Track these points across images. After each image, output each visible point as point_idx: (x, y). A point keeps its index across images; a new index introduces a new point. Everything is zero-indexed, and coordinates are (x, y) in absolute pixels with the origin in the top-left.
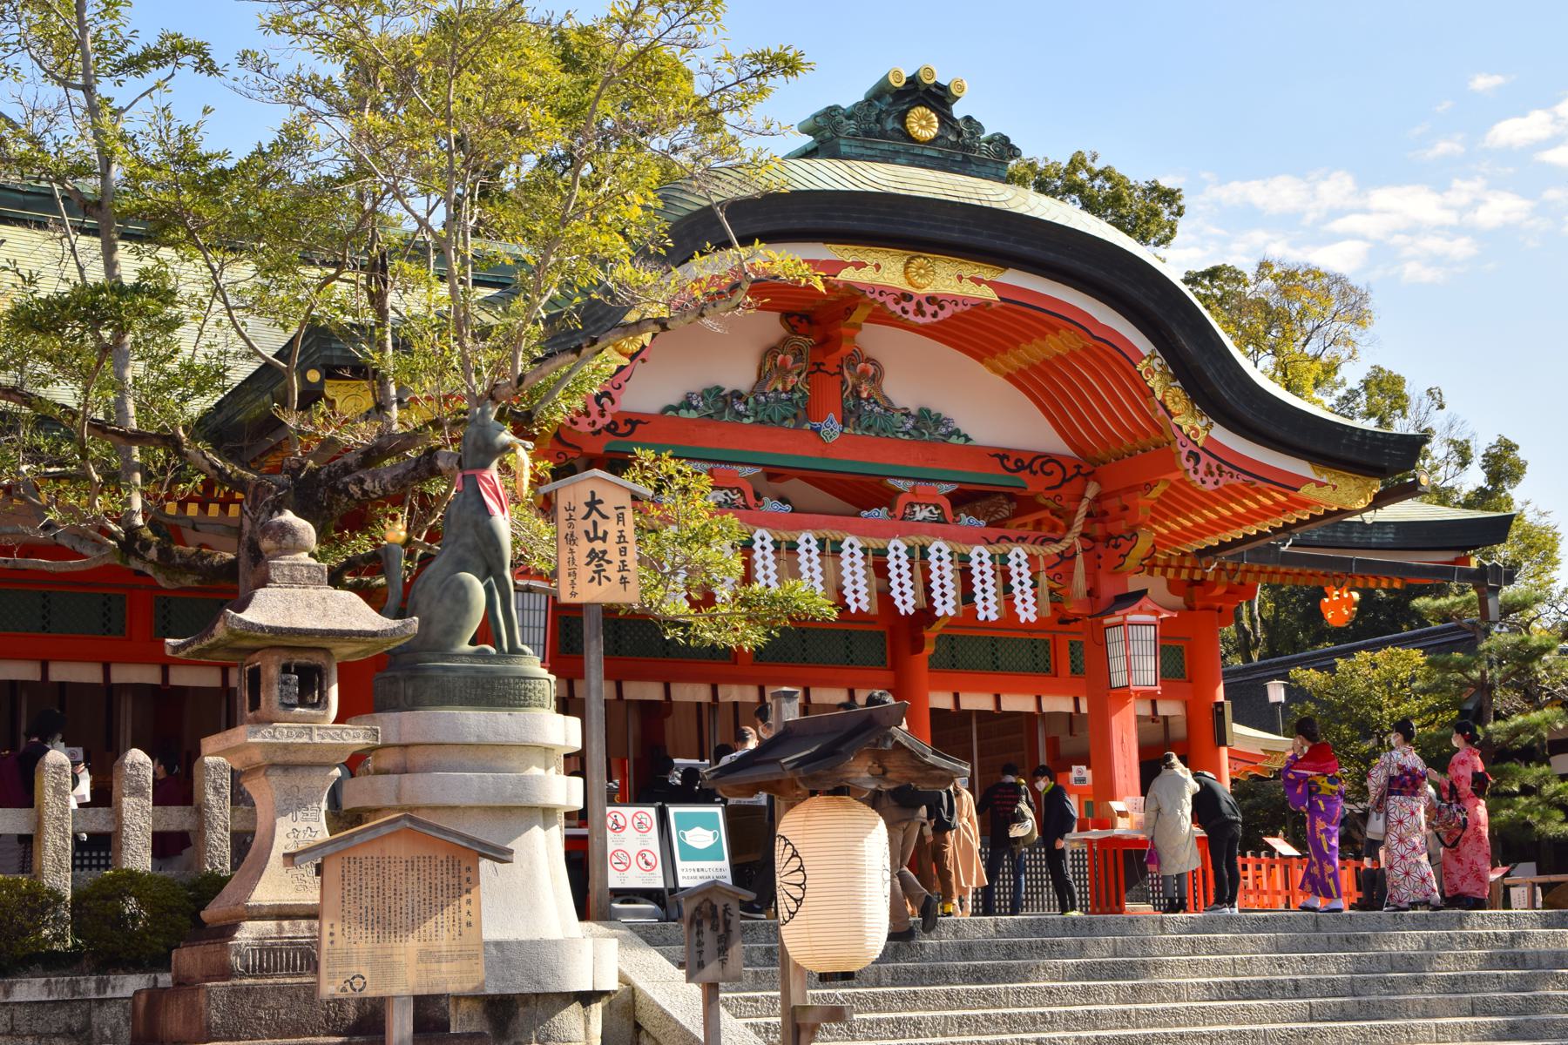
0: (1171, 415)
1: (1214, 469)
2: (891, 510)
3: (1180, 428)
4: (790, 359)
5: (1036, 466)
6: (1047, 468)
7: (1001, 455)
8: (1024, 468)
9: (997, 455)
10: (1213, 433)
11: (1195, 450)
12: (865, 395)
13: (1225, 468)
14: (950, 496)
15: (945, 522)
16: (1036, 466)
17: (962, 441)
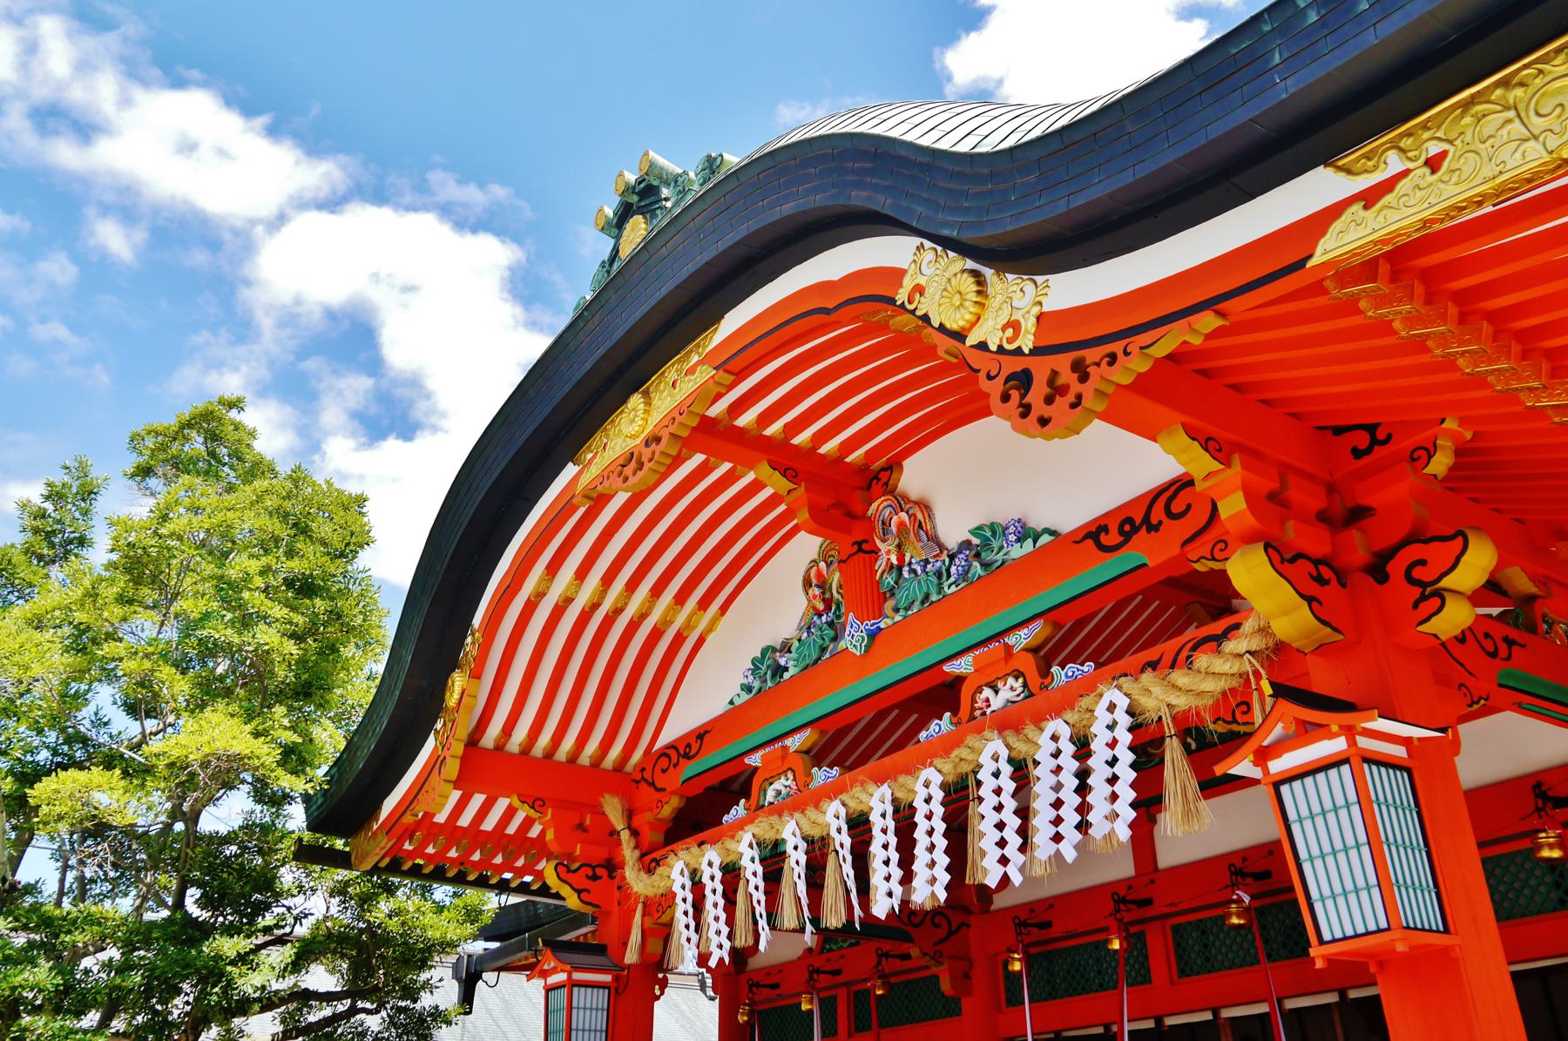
0: (960, 336)
1: (1067, 377)
2: (955, 713)
3: (983, 346)
4: (822, 565)
5: (1158, 514)
6: (1176, 507)
7: (1095, 534)
8: (1135, 529)
9: (1084, 538)
10: (1048, 307)
11: (1016, 365)
12: (894, 560)
13: (1091, 355)
14: (1033, 650)
15: (1031, 695)
16: (1158, 514)
17: (1028, 546)
